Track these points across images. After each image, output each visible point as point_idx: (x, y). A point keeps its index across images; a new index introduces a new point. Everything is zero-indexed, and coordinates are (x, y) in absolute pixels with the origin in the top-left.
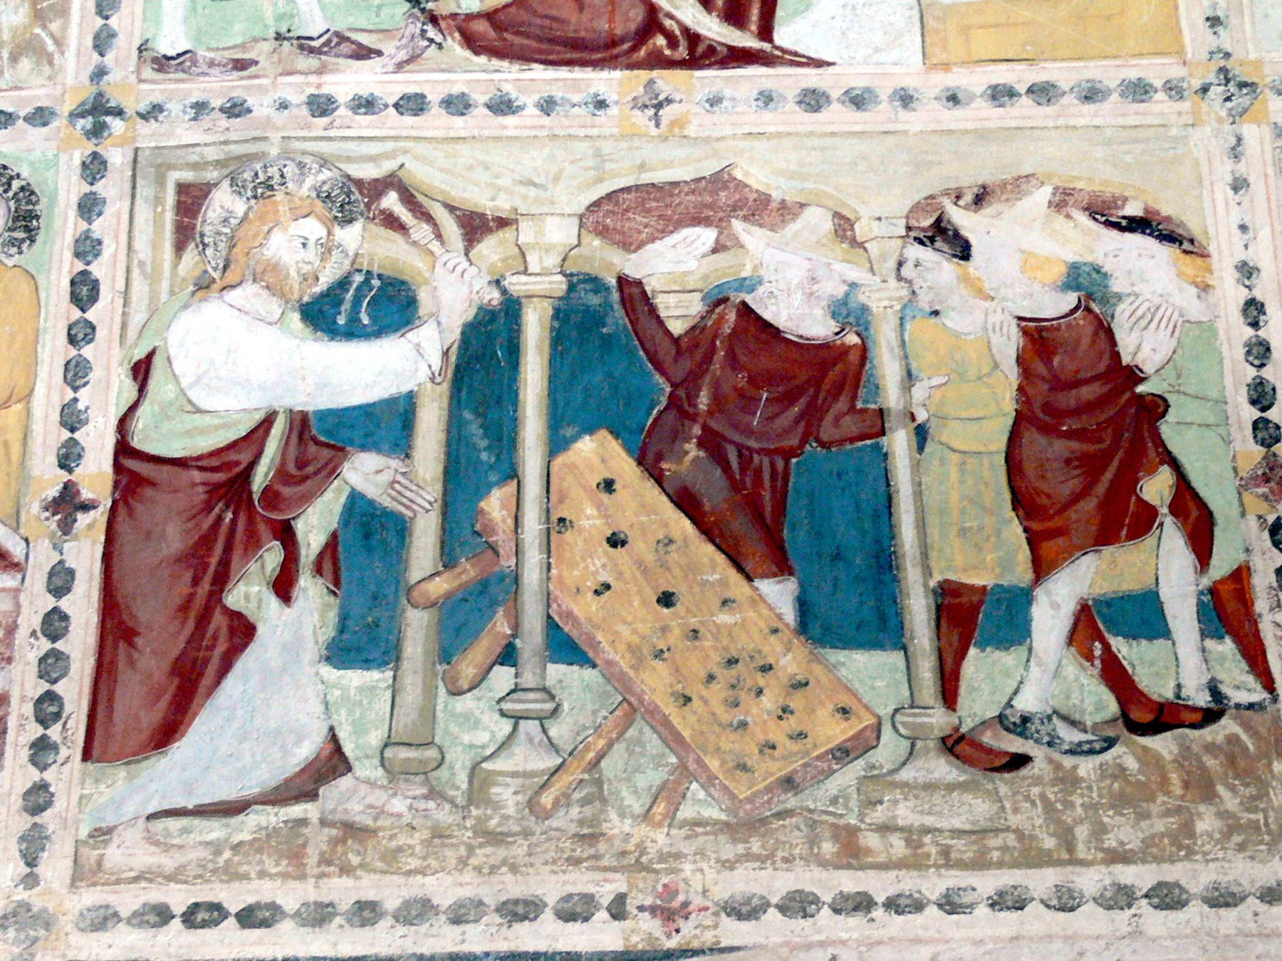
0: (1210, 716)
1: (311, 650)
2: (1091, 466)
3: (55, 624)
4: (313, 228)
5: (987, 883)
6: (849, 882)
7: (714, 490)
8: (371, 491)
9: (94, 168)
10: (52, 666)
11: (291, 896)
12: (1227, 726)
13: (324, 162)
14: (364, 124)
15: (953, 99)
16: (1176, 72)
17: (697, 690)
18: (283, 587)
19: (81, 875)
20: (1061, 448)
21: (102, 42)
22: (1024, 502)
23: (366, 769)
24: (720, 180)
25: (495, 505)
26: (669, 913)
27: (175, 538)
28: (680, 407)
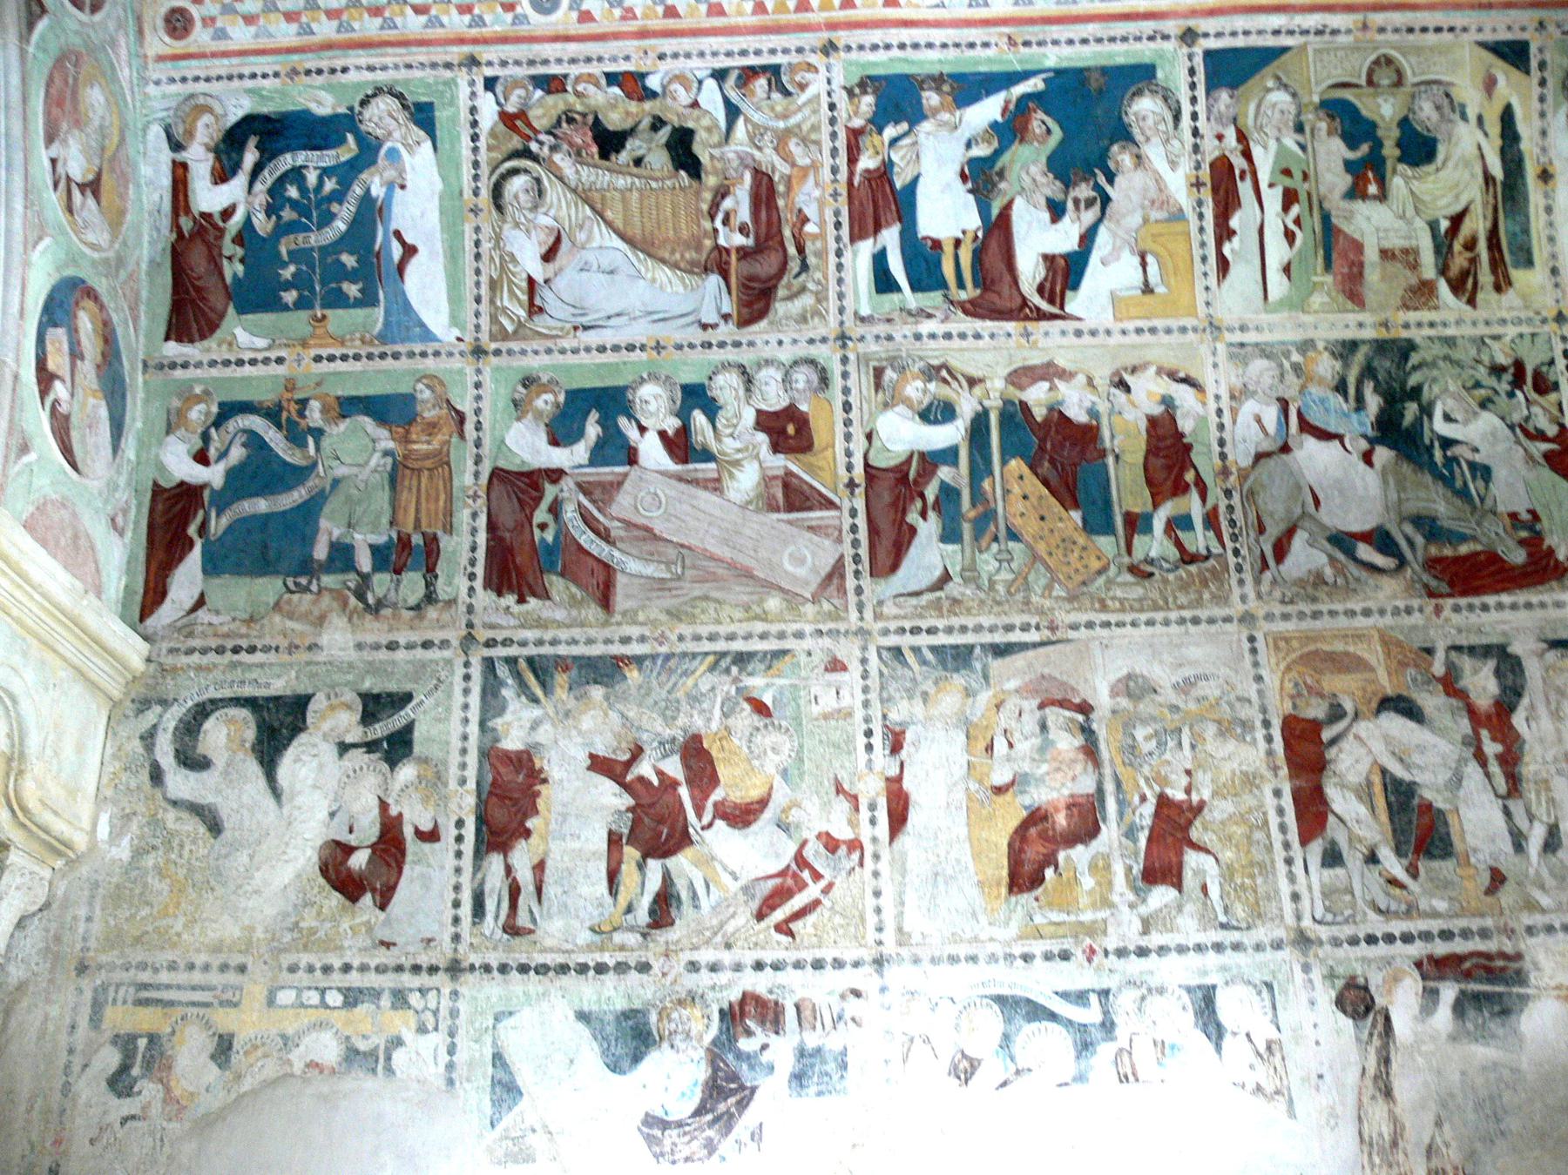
0: (1207, 558)
1: (935, 538)
2: (1169, 468)
4: (919, 384)
5: (1143, 617)
6: (1104, 617)
7: (1054, 481)
8: (947, 480)
9: (845, 360)
10: (855, 543)
11: (941, 624)
12: (1212, 562)
13: (921, 359)
14: (932, 344)
15: (1124, 332)
16: (1195, 322)
17: (1054, 551)
18: (924, 515)
19: (878, 616)
21: (841, 311)
22: (1150, 482)
23: (957, 579)
24: (1050, 364)
26: (1053, 628)
27: (887, 498)
28: (1042, 449)
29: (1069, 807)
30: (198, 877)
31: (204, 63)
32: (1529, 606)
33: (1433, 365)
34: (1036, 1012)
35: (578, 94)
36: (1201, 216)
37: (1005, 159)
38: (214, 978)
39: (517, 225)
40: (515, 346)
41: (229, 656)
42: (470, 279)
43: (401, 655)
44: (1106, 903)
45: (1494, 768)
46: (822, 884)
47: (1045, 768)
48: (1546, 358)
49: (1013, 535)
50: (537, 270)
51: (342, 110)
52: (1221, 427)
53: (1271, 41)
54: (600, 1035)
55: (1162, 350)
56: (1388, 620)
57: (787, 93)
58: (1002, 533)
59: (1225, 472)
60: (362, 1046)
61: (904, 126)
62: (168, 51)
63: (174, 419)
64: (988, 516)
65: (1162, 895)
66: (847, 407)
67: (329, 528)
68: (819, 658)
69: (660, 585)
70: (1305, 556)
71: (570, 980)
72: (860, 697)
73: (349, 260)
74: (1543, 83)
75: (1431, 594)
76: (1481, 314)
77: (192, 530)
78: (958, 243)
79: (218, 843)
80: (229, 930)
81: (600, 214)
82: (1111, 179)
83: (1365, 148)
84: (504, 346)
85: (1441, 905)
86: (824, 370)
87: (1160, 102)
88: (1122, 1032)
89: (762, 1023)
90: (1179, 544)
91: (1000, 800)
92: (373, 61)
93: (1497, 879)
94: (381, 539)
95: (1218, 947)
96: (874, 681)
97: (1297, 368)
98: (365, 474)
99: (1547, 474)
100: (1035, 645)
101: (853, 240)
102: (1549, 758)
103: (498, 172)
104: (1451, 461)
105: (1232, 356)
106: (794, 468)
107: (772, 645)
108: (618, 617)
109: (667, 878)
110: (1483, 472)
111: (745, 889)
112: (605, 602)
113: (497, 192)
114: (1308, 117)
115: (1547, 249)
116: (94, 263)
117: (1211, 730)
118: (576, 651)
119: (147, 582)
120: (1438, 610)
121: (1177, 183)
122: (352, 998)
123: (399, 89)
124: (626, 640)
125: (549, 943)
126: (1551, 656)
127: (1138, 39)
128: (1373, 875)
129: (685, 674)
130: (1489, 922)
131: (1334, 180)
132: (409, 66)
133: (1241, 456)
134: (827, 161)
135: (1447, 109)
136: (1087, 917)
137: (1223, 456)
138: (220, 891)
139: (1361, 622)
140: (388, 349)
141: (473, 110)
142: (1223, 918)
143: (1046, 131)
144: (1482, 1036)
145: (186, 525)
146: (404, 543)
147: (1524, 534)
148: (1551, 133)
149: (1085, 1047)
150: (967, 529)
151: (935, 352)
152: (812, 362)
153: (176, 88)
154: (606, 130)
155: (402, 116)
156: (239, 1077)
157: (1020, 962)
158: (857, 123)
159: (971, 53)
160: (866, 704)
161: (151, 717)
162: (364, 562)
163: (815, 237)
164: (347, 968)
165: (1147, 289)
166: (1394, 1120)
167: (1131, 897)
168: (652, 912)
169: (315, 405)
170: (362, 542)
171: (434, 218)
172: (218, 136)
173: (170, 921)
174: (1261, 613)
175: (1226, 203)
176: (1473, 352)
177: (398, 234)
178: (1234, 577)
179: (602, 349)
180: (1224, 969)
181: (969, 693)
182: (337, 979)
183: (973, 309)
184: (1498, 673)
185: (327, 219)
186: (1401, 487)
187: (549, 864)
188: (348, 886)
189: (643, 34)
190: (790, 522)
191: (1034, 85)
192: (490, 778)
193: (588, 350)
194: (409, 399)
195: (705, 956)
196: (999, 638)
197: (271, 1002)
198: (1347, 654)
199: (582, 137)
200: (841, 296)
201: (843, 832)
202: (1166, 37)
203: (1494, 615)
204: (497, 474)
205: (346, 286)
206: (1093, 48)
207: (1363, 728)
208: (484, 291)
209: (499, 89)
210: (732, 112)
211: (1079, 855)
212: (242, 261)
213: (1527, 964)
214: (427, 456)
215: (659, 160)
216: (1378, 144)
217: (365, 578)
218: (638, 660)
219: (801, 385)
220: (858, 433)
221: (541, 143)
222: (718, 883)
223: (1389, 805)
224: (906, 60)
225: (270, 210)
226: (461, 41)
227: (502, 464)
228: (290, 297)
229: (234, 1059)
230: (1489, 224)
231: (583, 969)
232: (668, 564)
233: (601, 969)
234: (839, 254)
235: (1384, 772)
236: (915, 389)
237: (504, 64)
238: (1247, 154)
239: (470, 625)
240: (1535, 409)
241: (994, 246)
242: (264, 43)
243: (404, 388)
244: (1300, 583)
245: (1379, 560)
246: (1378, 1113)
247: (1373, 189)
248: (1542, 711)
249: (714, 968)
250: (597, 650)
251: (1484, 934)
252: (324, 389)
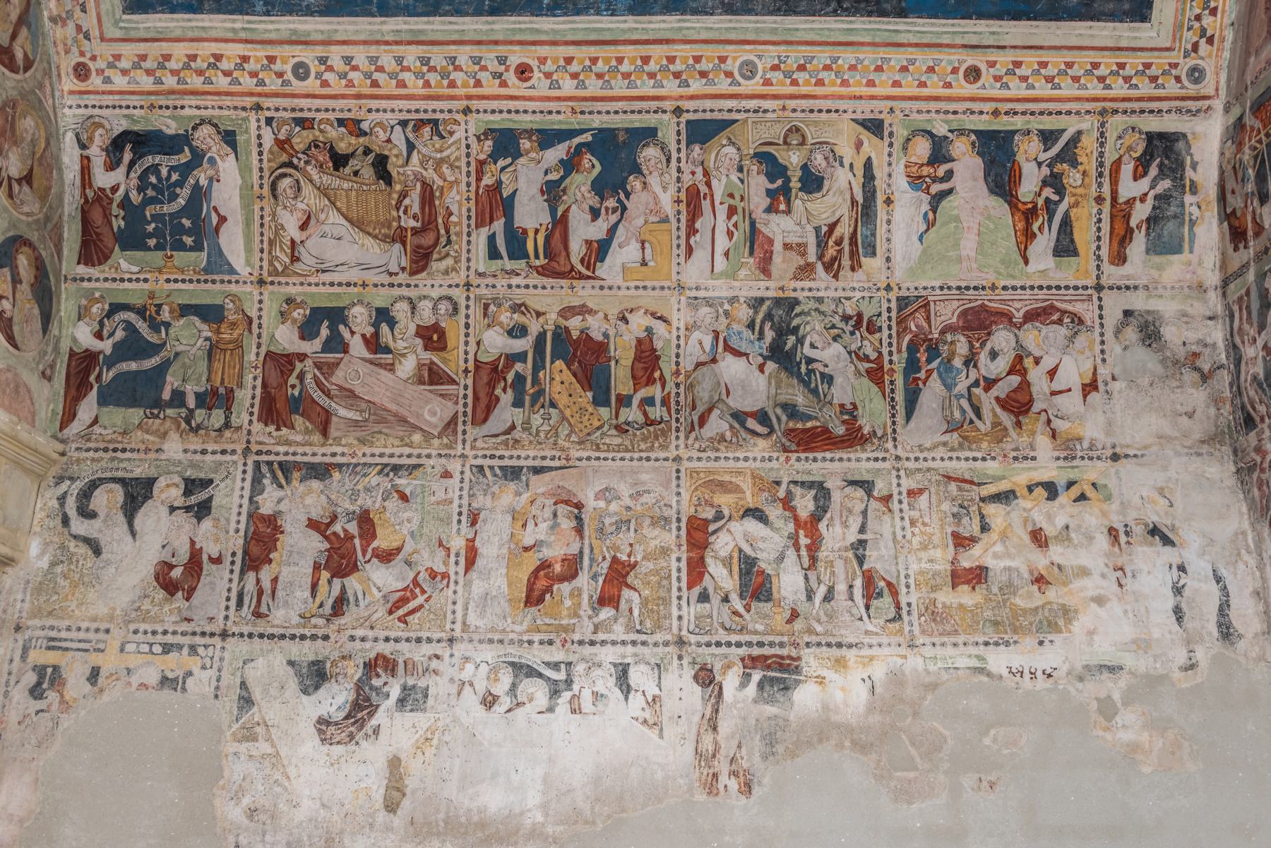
2: (646, 369)
3: (465, 396)
4: (508, 314)
6: (597, 454)
7: (580, 374)
9: (468, 298)
10: (465, 405)
11: (507, 453)
14: (518, 291)
18: (504, 390)
19: (473, 448)
20: (641, 365)
21: (468, 268)
22: (634, 377)
23: (519, 428)
24: (584, 306)
25: (541, 374)
26: (568, 459)
27: (485, 379)
28: (574, 355)
29: (563, 560)
30: (86, 579)
31: (98, 97)
32: (841, 460)
33: (808, 314)
34: (532, 672)
35: (321, 131)
36: (679, 220)
37: (568, 181)
38: (91, 636)
39: (285, 207)
40: (283, 280)
41: (111, 454)
42: (257, 238)
43: (209, 457)
44: (576, 615)
45: (804, 552)
46: (426, 596)
47: (553, 538)
48: (875, 311)
49: (553, 405)
50: (297, 236)
51: (181, 132)
52: (678, 346)
53: (727, 116)
54: (299, 674)
55: (649, 300)
56: (758, 464)
57: (442, 137)
58: (547, 404)
59: (677, 373)
60: (170, 675)
61: (509, 160)
62: (77, 88)
63: (82, 311)
64: (541, 392)
65: (606, 613)
66: (467, 326)
67: (172, 381)
68: (438, 470)
69: (356, 424)
70: (718, 424)
71: (286, 643)
72: (457, 493)
73: (187, 223)
74: (891, 145)
75: (786, 450)
76: (840, 284)
77: (92, 378)
78: (537, 231)
79: (99, 562)
80: (101, 609)
81: (333, 203)
82: (627, 197)
83: (779, 182)
84: (277, 279)
85: (760, 627)
86: (456, 304)
87: (659, 151)
88: (576, 687)
89: (386, 671)
90: (645, 414)
91: (526, 554)
92: (199, 103)
93: (794, 615)
95: (634, 643)
96: (466, 485)
97: (727, 313)
98: (194, 351)
99: (866, 381)
100: (557, 469)
101: (477, 227)
102: (836, 548)
104: (810, 372)
105: (689, 305)
106: (435, 360)
107: (413, 461)
108: (331, 441)
109: (343, 588)
110: (828, 379)
111: (384, 596)
112: (325, 432)
113: (274, 187)
114: (746, 162)
115: (885, 246)
116: (29, 224)
117: (648, 521)
118: (306, 459)
119: (64, 408)
120: (788, 459)
121: (666, 201)
122: (167, 649)
124: (334, 455)
125: (276, 622)
126: (848, 490)
127: (648, 112)
128: (725, 609)
129: (365, 475)
130: (785, 639)
131: (759, 201)
132: (221, 108)
133: (687, 364)
134: (465, 179)
135: (831, 160)
136: (564, 622)
137: (677, 364)
138: (97, 586)
139: (741, 464)
140: (209, 277)
141: (259, 137)
142: (638, 627)
143: (592, 166)
144: (771, 701)
145: (89, 376)
146: (214, 392)
147: (846, 417)
148: (894, 175)
149: (555, 693)
150: (527, 398)
151: (519, 296)
152: (449, 298)
153: (82, 111)
154: (337, 153)
155: (217, 138)
156: (101, 691)
157: (526, 645)
158: (482, 157)
159: (549, 117)
160: (460, 497)
161: (64, 487)
162: (191, 402)
163: (456, 224)
164: (165, 633)
165: (644, 263)
166: (716, 743)
167: (590, 612)
168: (333, 607)
169: (166, 308)
170: (190, 389)
171: (236, 201)
172: (108, 142)
173: (68, 603)
174: (686, 456)
175: (694, 212)
176: (833, 307)
177: (215, 209)
178: (674, 434)
179: (332, 284)
180: (636, 655)
181: (518, 494)
182: (159, 638)
183: (543, 271)
184: (815, 498)
185: (173, 197)
186: (778, 387)
187: (281, 578)
188: (170, 587)
189: (358, 96)
190: (430, 391)
191: (587, 137)
192: (252, 529)
193: (324, 284)
194: (220, 308)
195: (360, 633)
196: (538, 463)
197: (122, 650)
198: (731, 482)
199: (323, 157)
200: (469, 260)
201: (440, 568)
202: (664, 112)
203: (820, 464)
204: (269, 355)
205: (184, 238)
206: (621, 116)
207: (735, 526)
208: (265, 246)
209: (274, 125)
210: (411, 147)
211: (565, 588)
212: (123, 218)
213: (803, 664)
214: (230, 342)
215: (368, 173)
216: (788, 180)
217: (191, 411)
218: (339, 466)
219: (442, 312)
220: (472, 340)
222: (371, 593)
223: (740, 569)
224: (511, 120)
225: (140, 189)
226: (251, 94)
227: (272, 348)
228: (152, 242)
229: (101, 680)
230: (851, 229)
231: (293, 637)
232: (361, 411)
233: (303, 637)
234: (469, 234)
235: (740, 551)
236: (505, 317)
237: (277, 110)
238: (708, 184)
239: (248, 442)
240: (866, 343)
241: (557, 235)
242: (133, 87)
243: (218, 302)
244: (711, 440)
245: (759, 429)
246: (708, 740)
247: (782, 207)
248: (837, 522)
249: (363, 640)
250: (318, 459)
251: (782, 645)
252: (170, 299)
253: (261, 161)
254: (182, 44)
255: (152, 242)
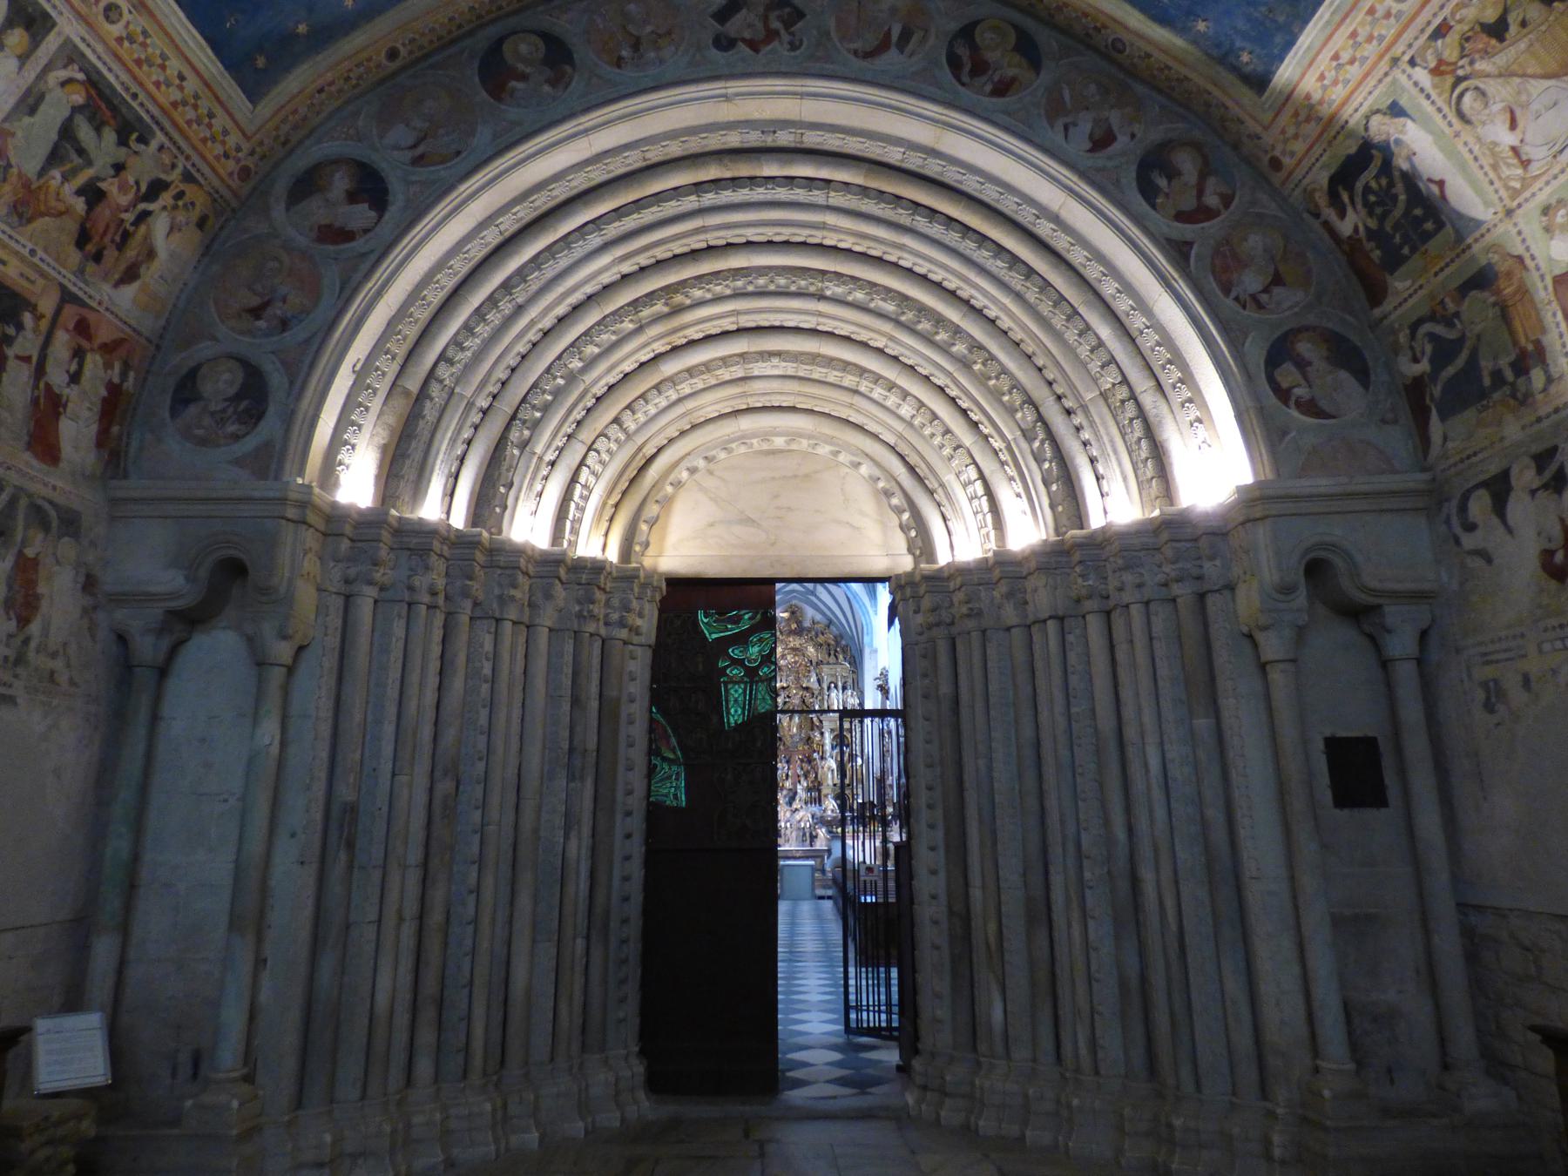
35: (1460, 21)
39: (1484, 123)
40: (1527, 194)
42: (1480, 174)
81: (1524, 75)
84: (1520, 199)
94: (1513, 357)
103: (1453, 102)
113: (1461, 115)
123: (1375, 108)
132: (1370, 93)
141: (1416, 84)
145: (1424, 400)
155: (1387, 119)
169: (1447, 300)
177: (1430, 180)
185: (1395, 198)
199: (1483, 41)
208: (1492, 175)
209: (1418, 60)
214: (1515, 293)
221: (1462, 67)
226: (1382, 56)
227: (1558, 272)
228: (1406, 251)
237: (1410, 46)
242: (1309, 141)
253: (1433, 103)
254: (1307, 76)
255: (1406, 251)
